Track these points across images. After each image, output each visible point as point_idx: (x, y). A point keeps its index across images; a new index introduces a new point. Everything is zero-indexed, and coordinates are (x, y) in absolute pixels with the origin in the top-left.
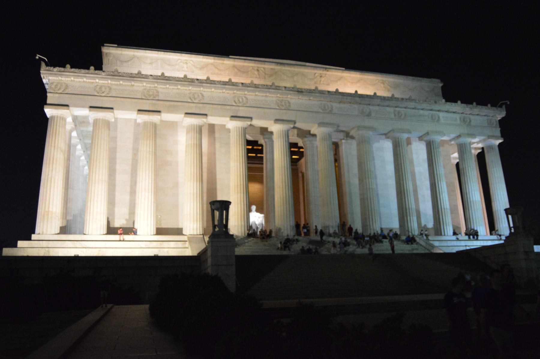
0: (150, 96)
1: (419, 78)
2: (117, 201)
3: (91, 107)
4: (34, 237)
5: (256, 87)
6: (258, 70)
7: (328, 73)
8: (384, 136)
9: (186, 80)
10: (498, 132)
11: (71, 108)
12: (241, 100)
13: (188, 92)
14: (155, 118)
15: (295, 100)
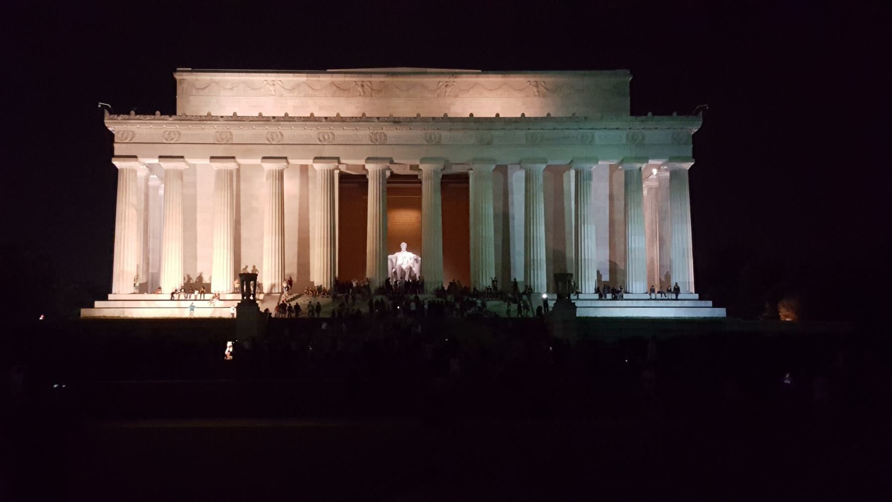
0: (222, 139)
1: (594, 72)
2: (199, 254)
3: (160, 157)
4: (110, 297)
5: (343, 121)
6: (363, 86)
7: (457, 80)
8: (518, 166)
9: (262, 119)
10: (689, 150)
11: (140, 159)
12: (326, 137)
13: (266, 132)
14: (230, 165)
15: (392, 133)
